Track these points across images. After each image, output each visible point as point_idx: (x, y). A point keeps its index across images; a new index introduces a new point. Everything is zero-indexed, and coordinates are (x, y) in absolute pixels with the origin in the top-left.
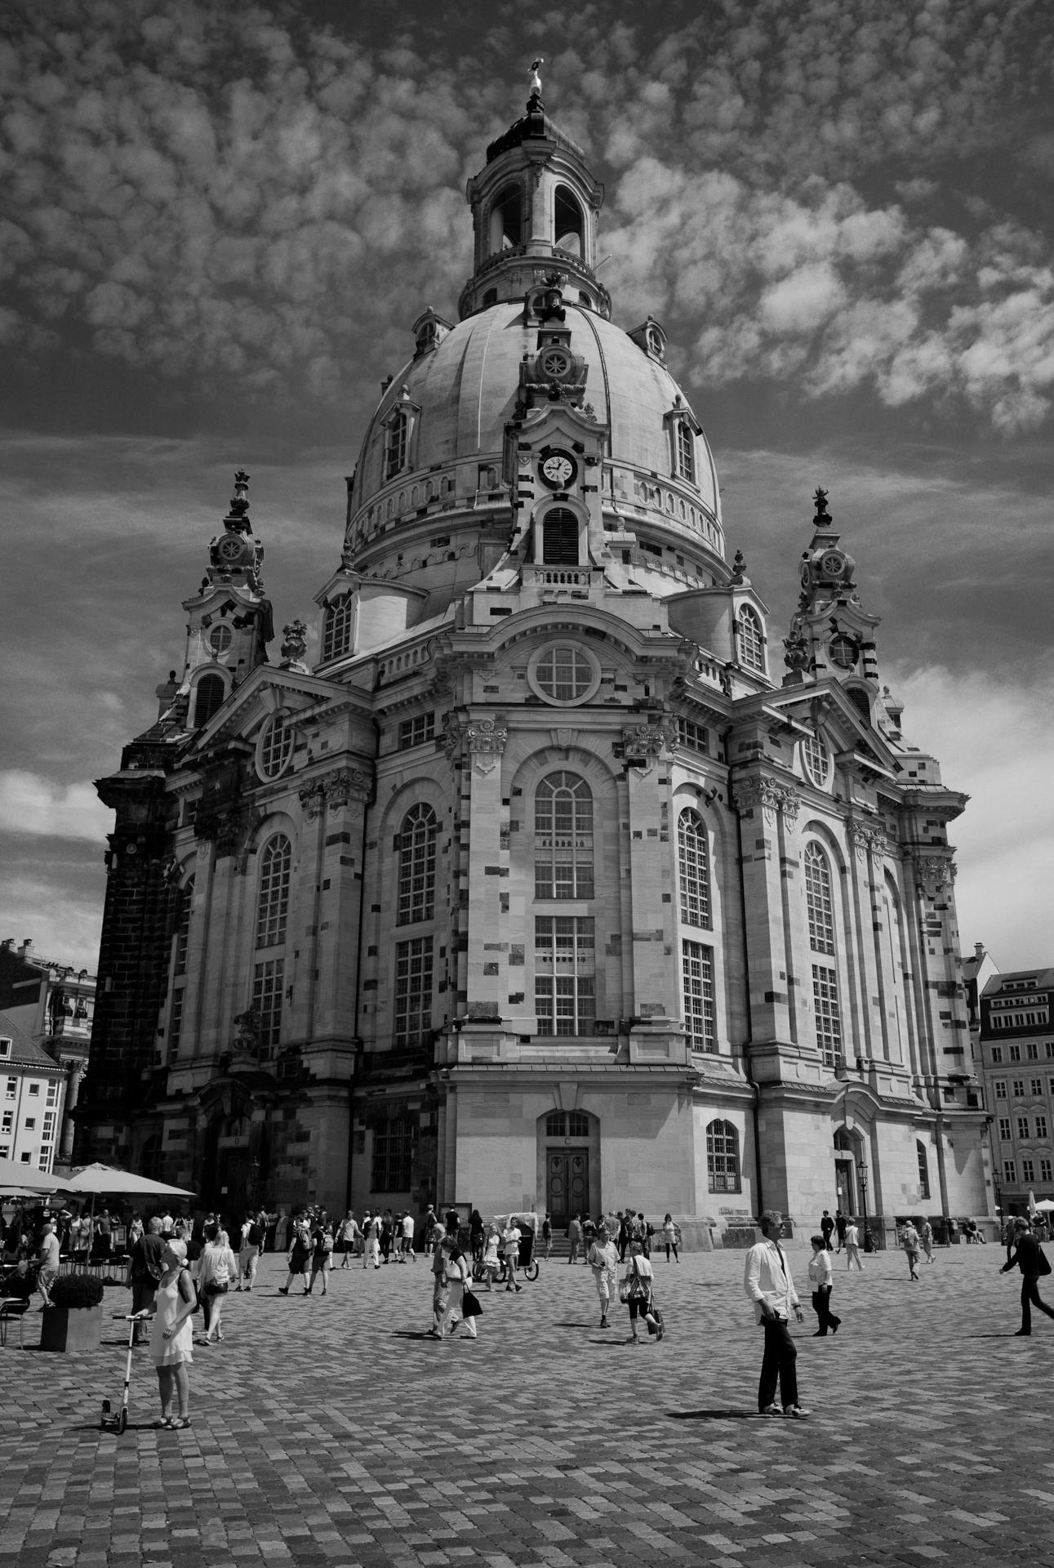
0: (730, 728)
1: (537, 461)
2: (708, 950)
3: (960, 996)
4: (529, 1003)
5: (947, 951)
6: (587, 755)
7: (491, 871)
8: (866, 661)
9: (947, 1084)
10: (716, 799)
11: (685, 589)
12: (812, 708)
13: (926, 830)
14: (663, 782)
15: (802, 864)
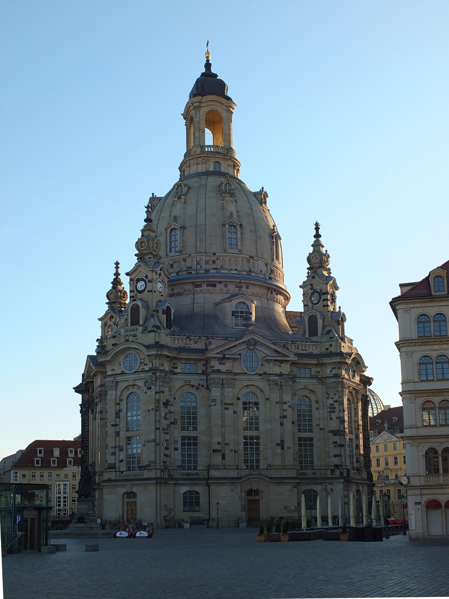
0: (207, 361)
1: (135, 284)
2: (195, 438)
3: (341, 435)
4: (124, 462)
5: (337, 418)
6: (139, 387)
7: (112, 425)
8: (324, 300)
9: (333, 468)
10: (200, 387)
11: (229, 295)
12: (247, 344)
13: (331, 371)
14: (157, 393)
15: (241, 402)
